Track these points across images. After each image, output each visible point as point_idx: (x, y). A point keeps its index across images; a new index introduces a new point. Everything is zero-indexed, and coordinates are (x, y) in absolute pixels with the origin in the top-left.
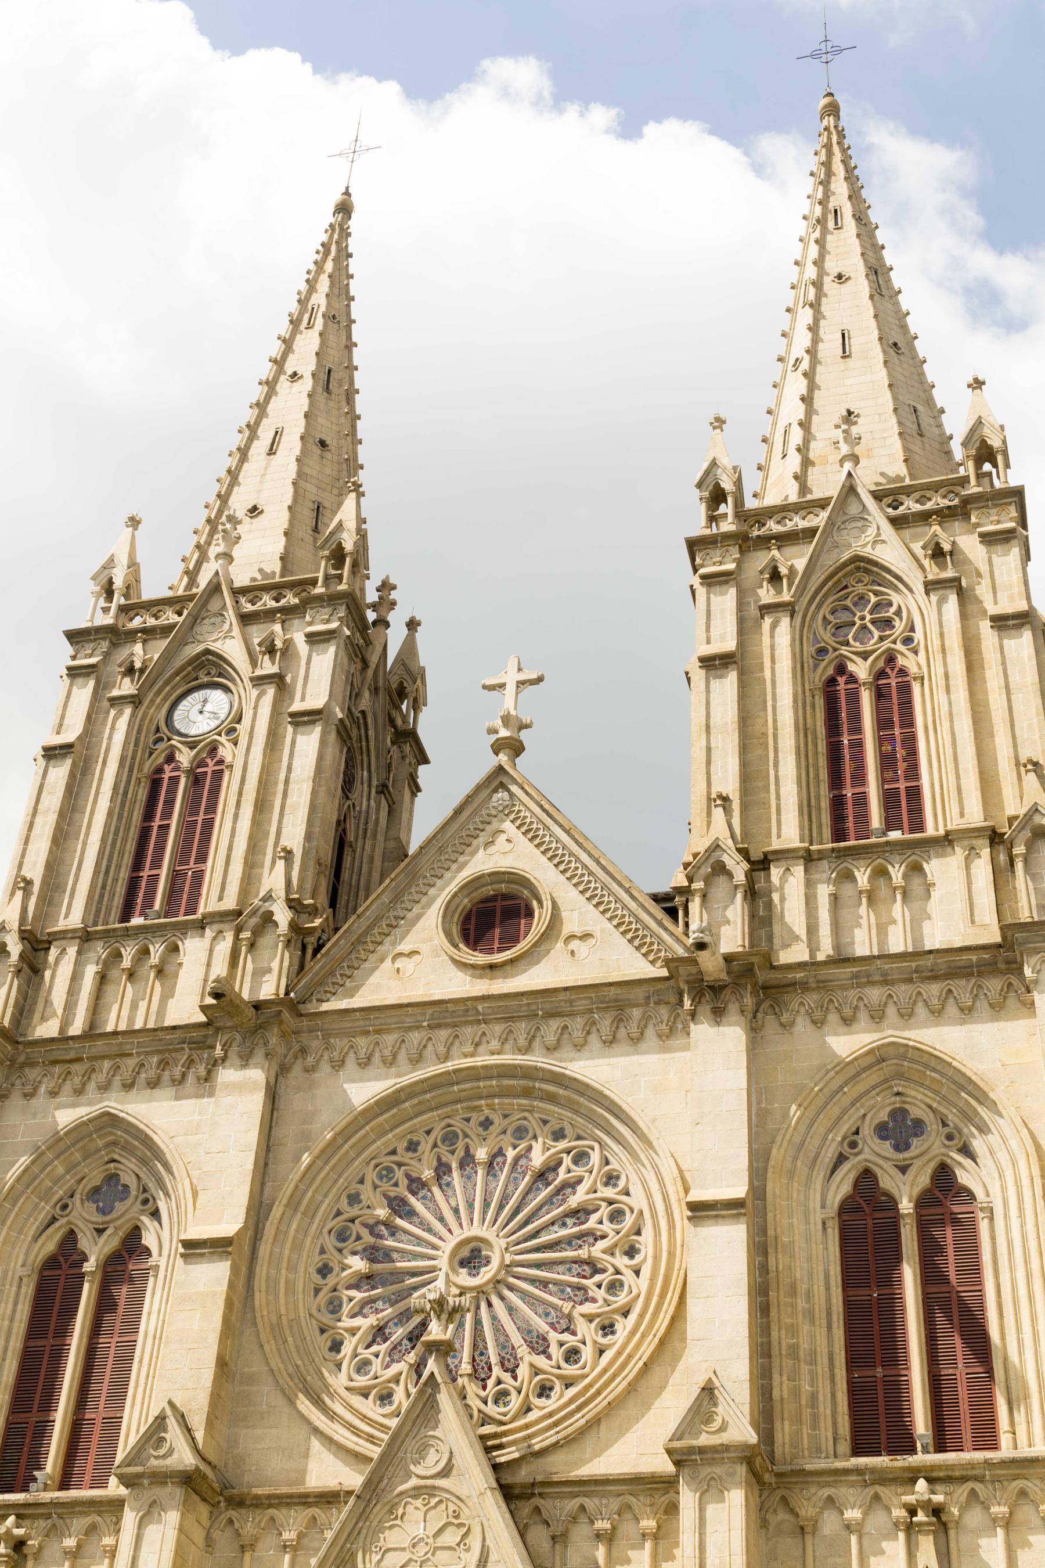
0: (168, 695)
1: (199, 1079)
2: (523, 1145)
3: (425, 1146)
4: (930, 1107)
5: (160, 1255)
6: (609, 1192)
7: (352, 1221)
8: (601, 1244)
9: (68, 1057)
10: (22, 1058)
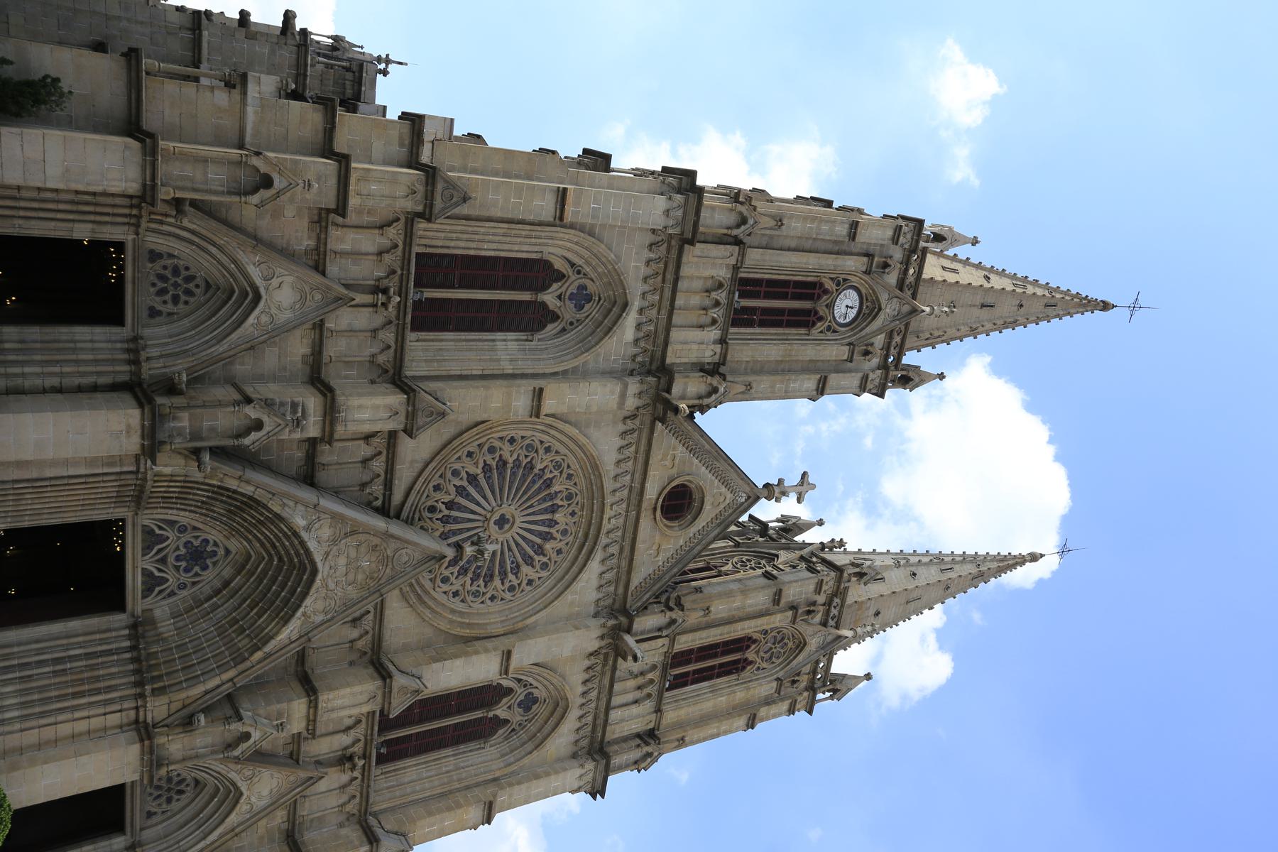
1: (635, 356)
2: (558, 536)
3: (569, 484)
4: (536, 715)
5: (539, 340)
7: (537, 451)
9: (667, 274)
10: (673, 243)
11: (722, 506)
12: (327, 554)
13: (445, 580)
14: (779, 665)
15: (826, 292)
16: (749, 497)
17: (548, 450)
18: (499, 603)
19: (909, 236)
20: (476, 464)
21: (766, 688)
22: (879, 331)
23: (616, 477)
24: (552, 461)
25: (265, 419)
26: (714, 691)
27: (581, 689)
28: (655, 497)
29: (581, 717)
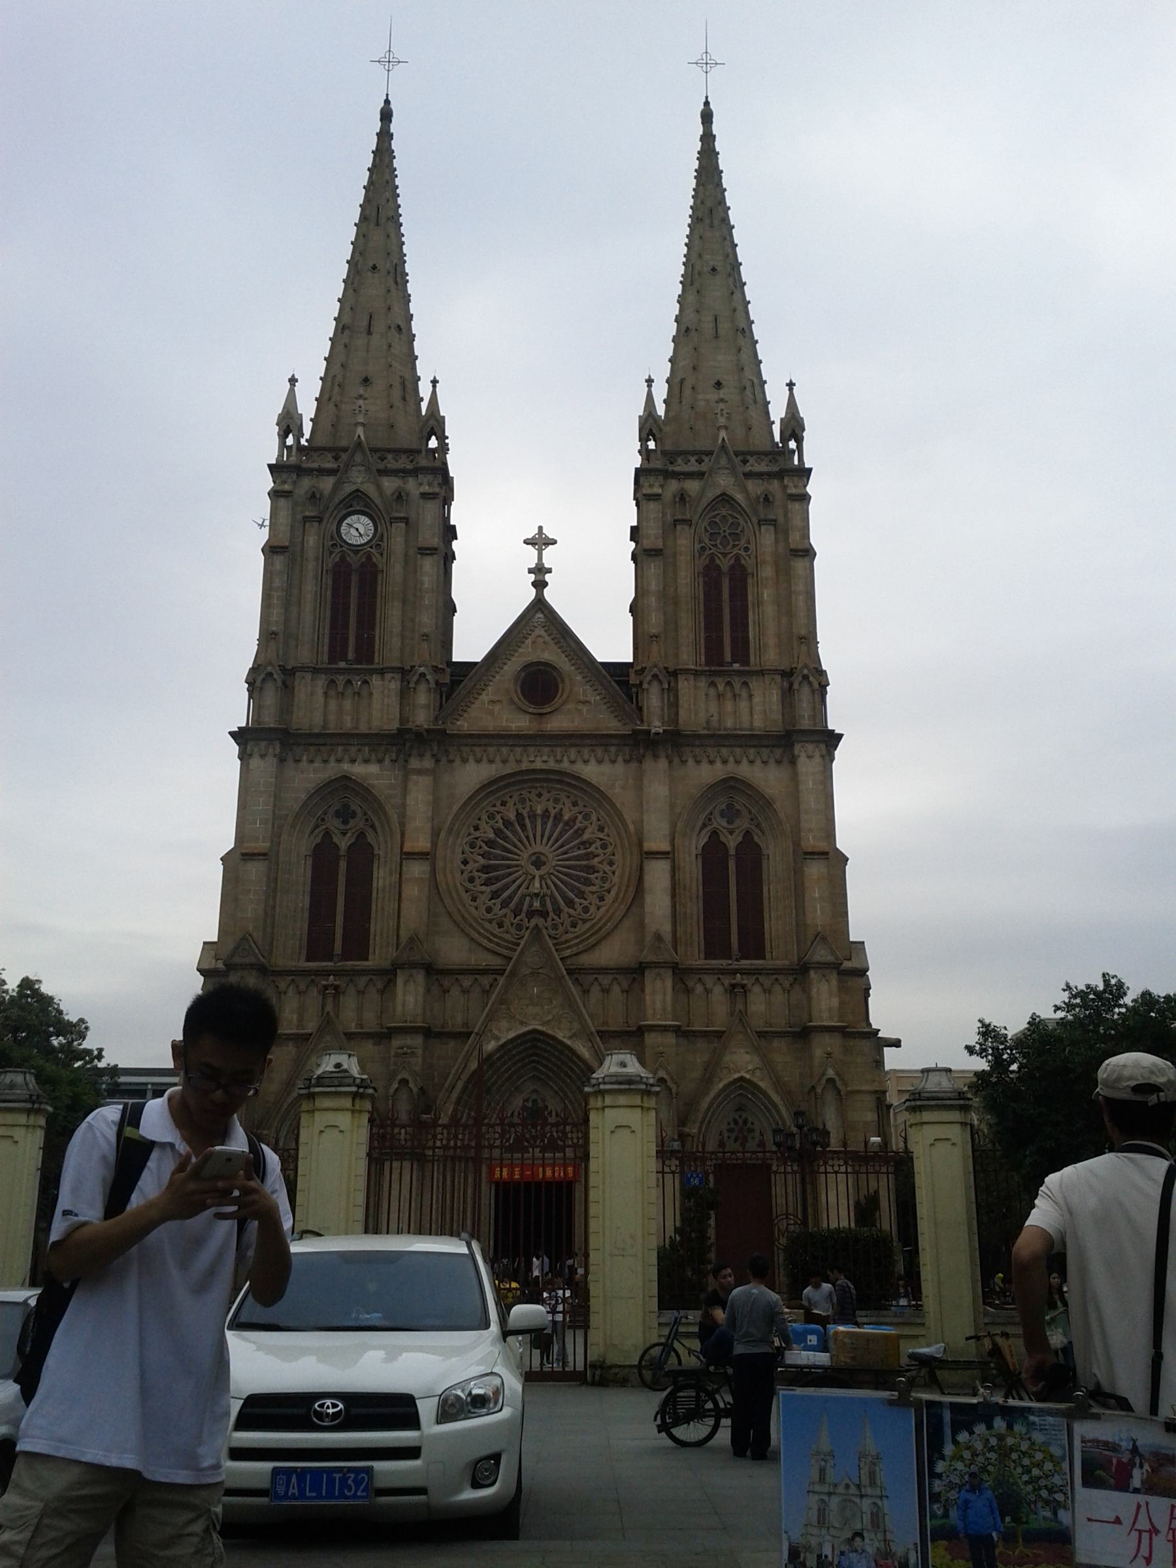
2: (558, 807)
3: (510, 803)
6: (601, 835)
7: (477, 839)
8: (596, 860)
10: (291, 741)
11: (548, 638)
12: (522, 1023)
13: (586, 910)
14: (746, 522)
15: (343, 559)
16: (540, 609)
17: (476, 828)
18: (616, 858)
19: (284, 476)
20: (482, 893)
21: (767, 539)
22: (379, 487)
23: (504, 762)
24: (487, 823)
25: (399, 1077)
26: (759, 603)
27: (718, 765)
28: (528, 716)
29: (752, 762)
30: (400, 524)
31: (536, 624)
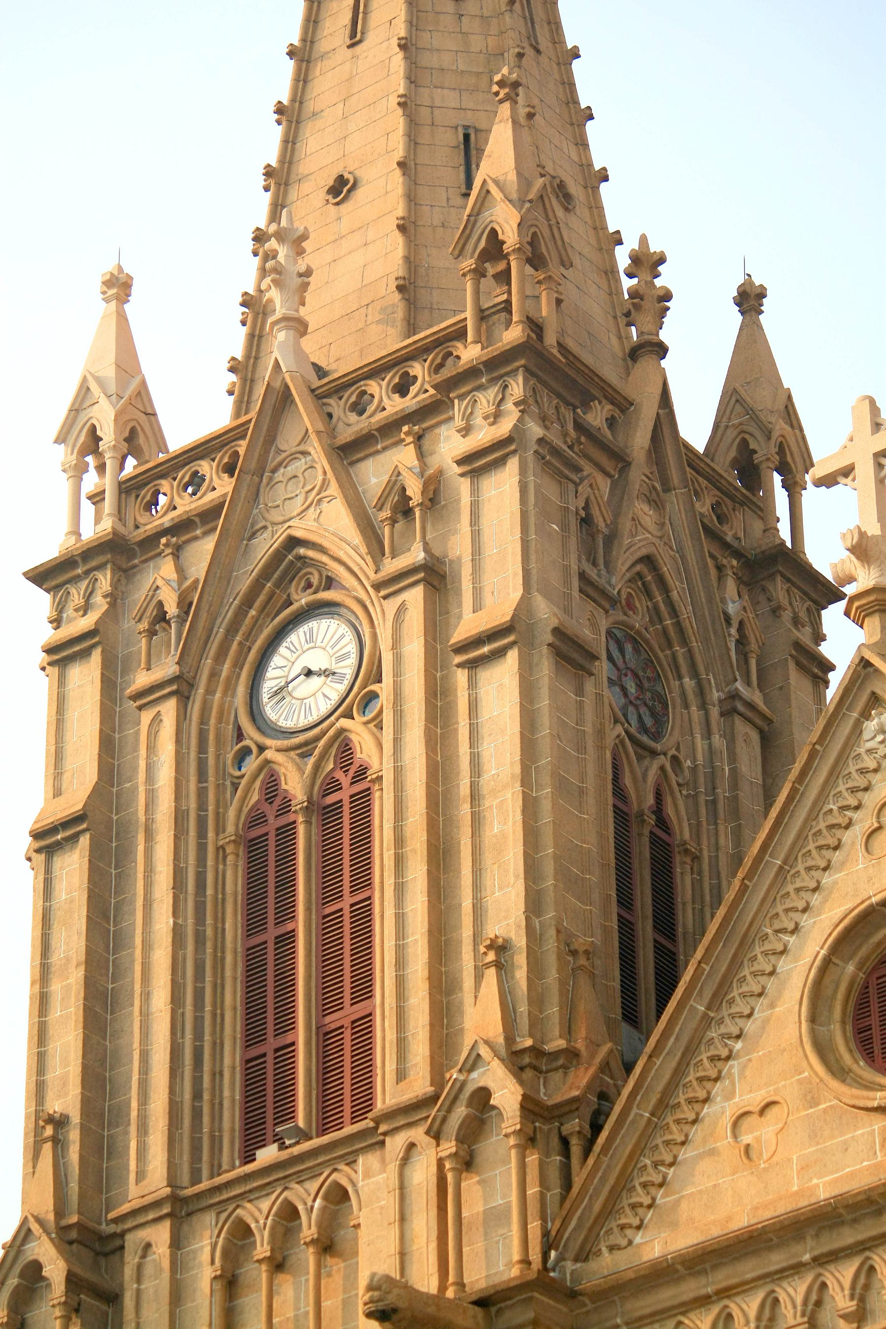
0: (244, 650)
30: (406, 596)
31: (872, 765)
